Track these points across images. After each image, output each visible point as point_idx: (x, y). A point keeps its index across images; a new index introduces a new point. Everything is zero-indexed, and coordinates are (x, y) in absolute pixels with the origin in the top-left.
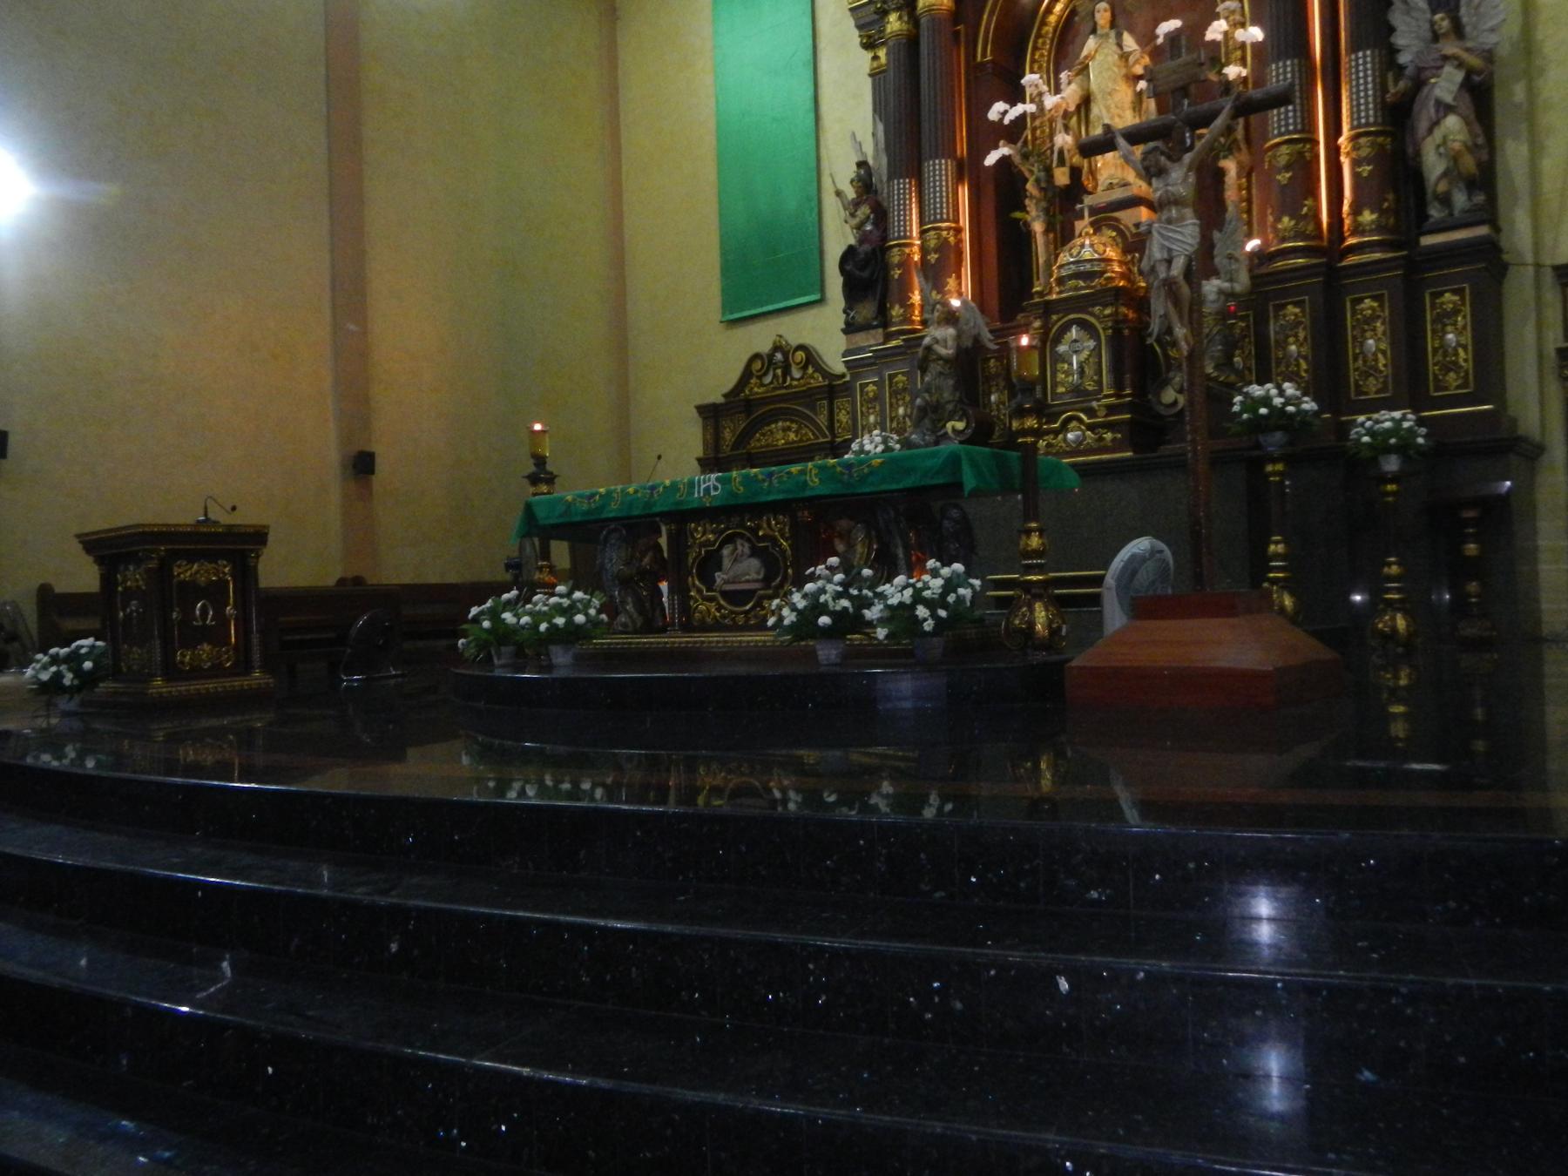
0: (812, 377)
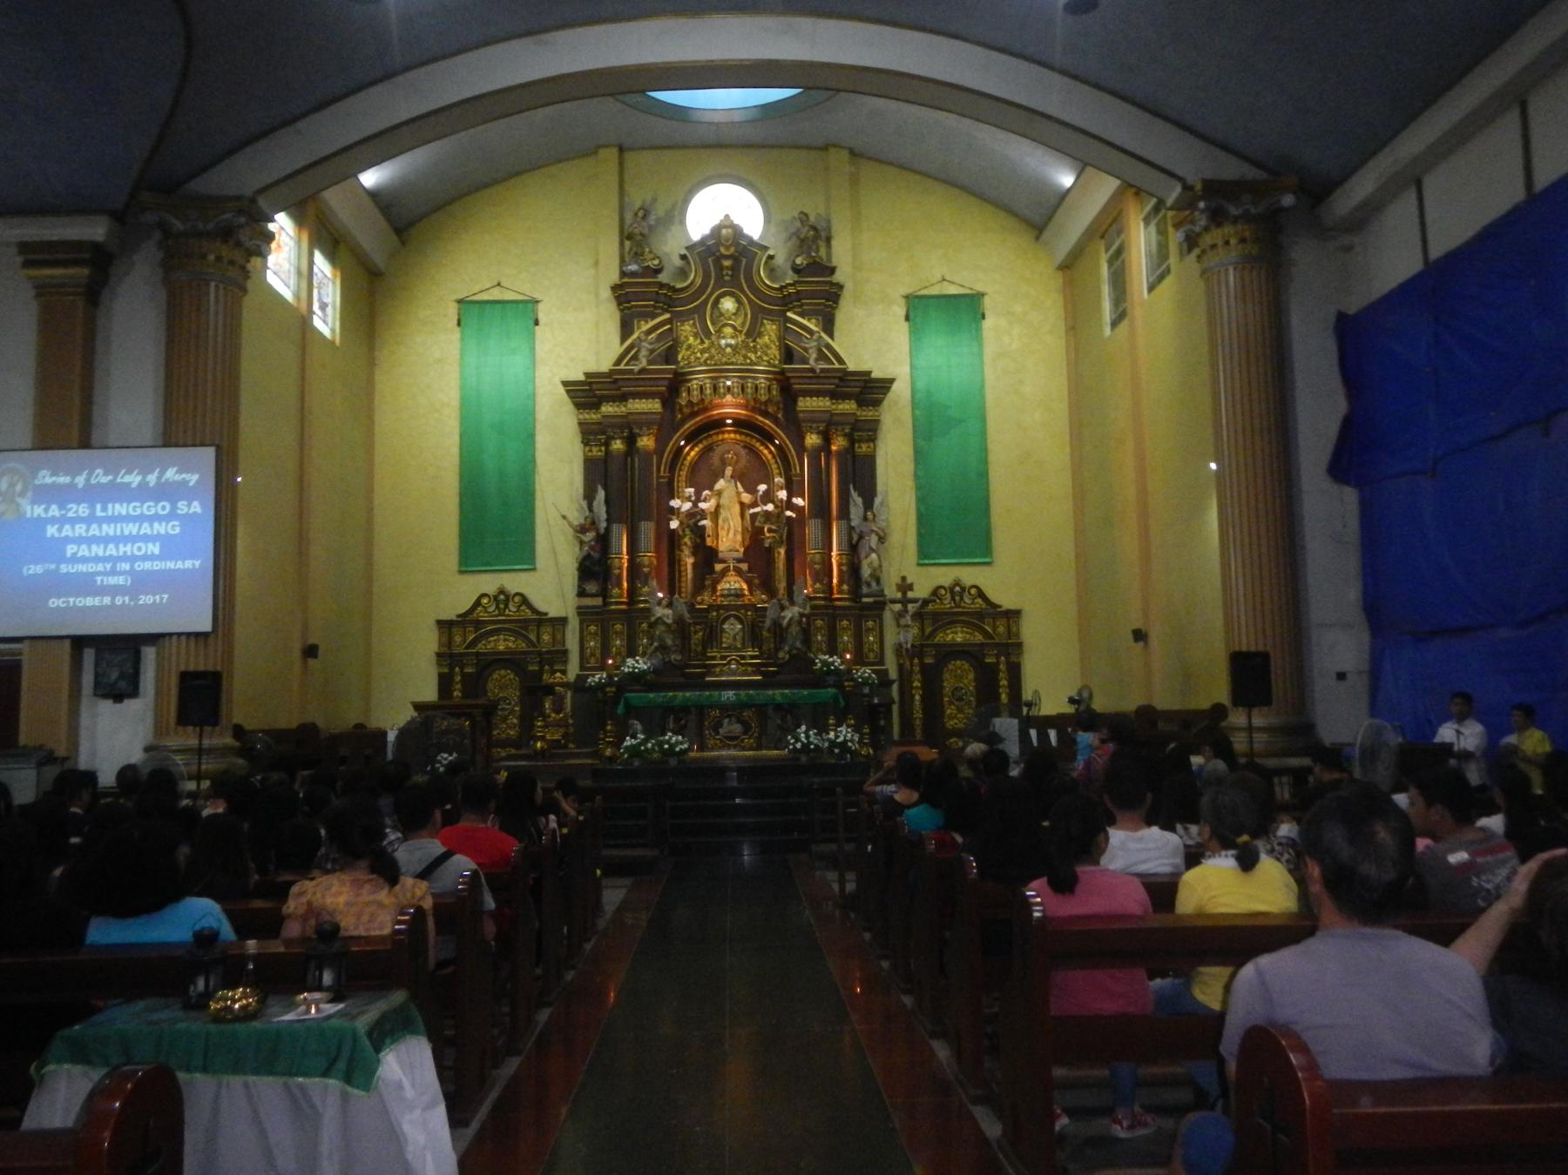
0: (523, 611)
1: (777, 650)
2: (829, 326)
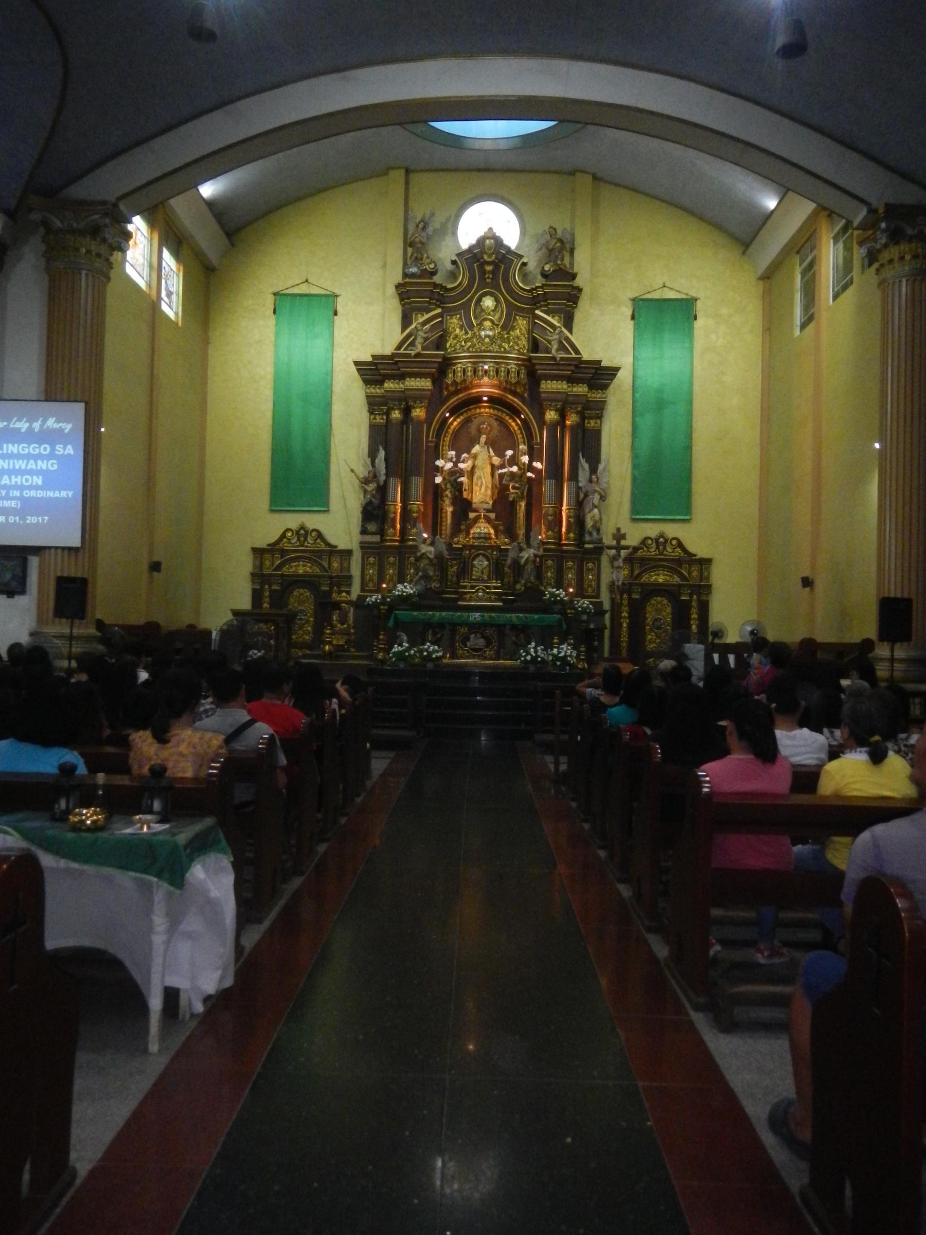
1: (516, 582)
2: (569, 323)
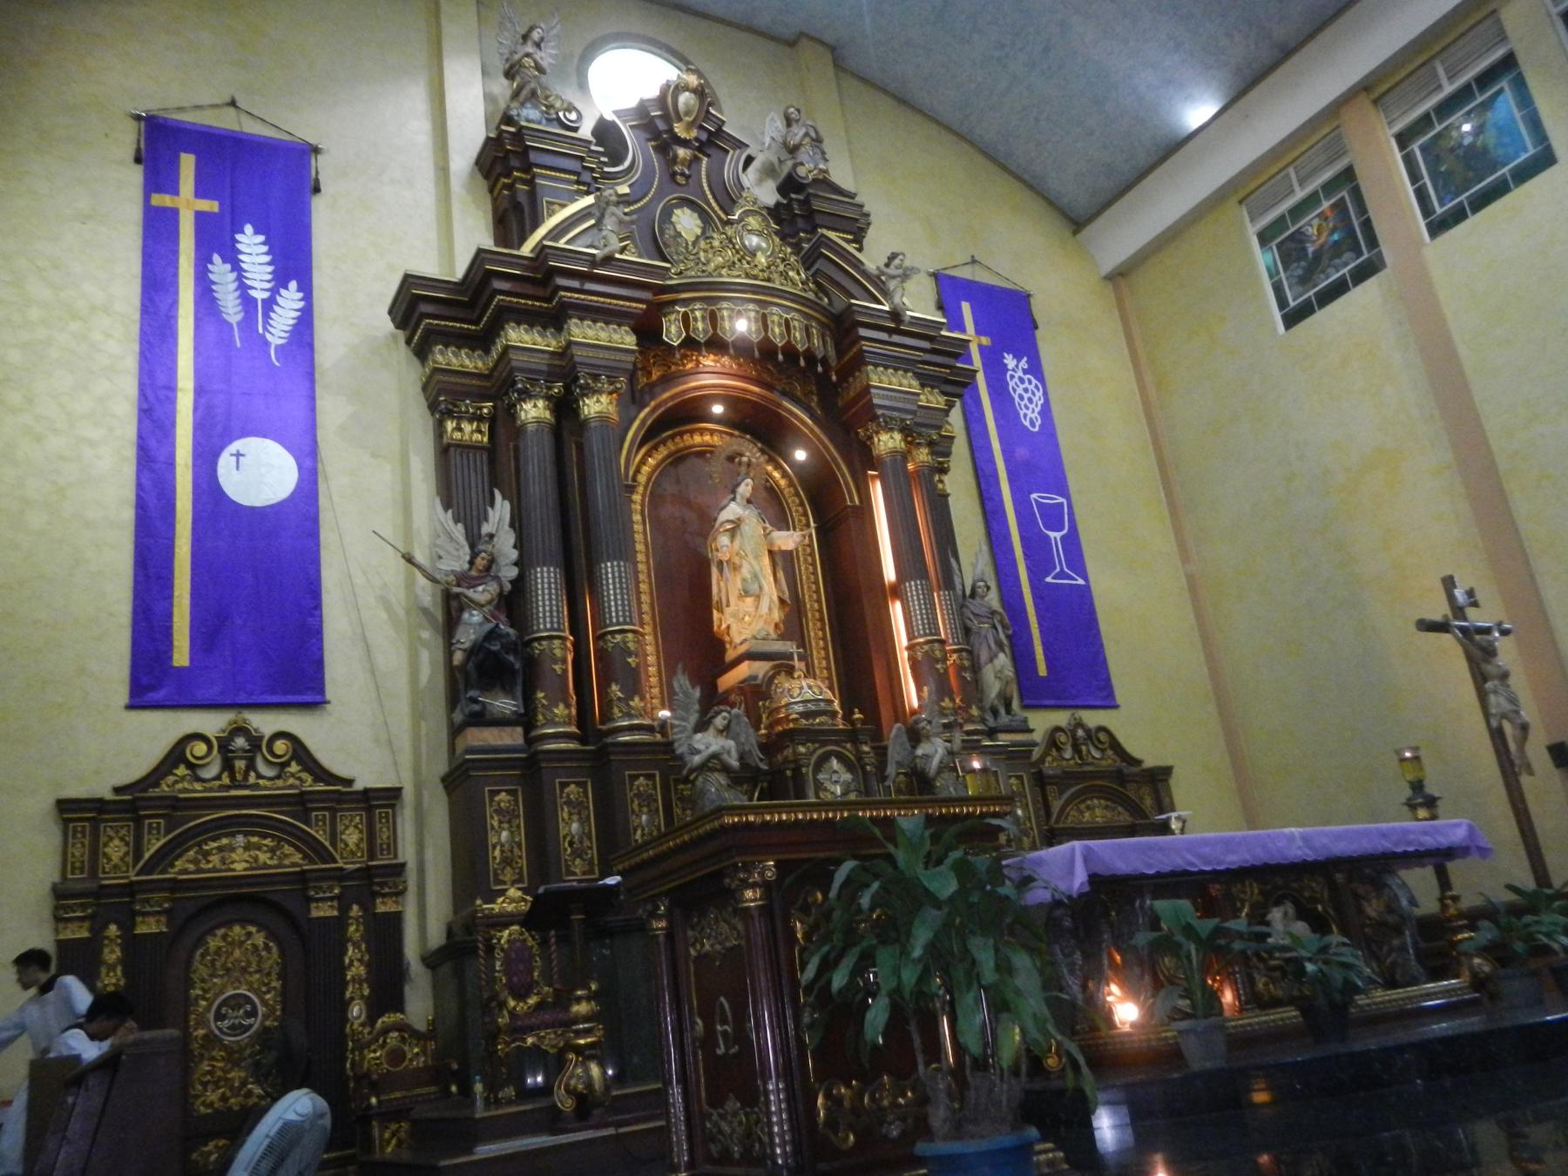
0: (293, 775)
